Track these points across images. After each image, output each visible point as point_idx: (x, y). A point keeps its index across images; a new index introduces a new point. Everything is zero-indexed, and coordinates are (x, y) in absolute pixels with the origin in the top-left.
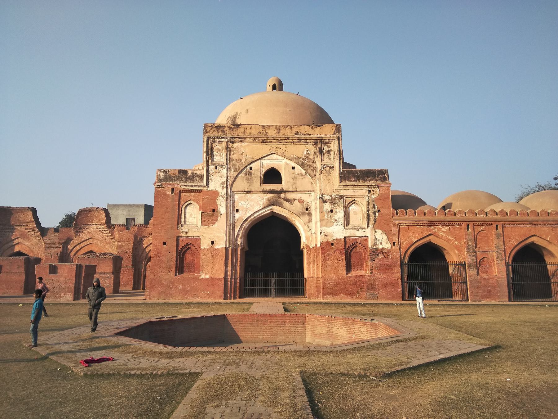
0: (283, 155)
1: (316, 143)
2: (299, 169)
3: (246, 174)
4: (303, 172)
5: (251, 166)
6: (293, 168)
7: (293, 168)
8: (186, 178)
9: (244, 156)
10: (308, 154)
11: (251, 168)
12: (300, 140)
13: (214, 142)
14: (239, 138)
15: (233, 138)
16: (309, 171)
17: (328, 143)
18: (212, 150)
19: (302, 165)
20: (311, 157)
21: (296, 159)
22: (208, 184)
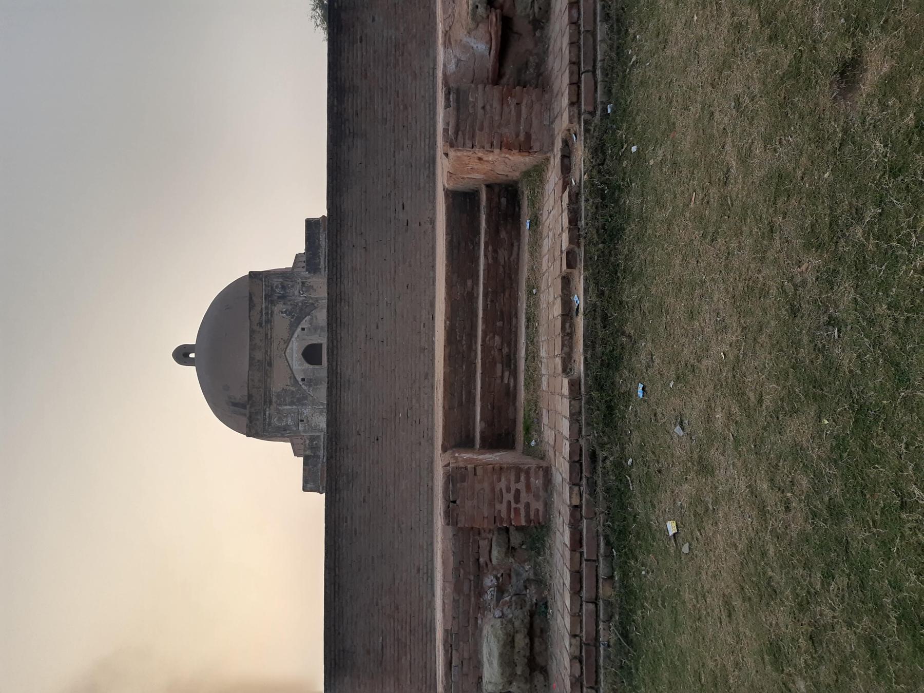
0: (288, 342)
1: (272, 303)
2: (305, 324)
3: (310, 386)
4: (307, 318)
5: (300, 380)
6: (303, 329)
7: (303, 329)
8: (313, 457)
9: (288, 388)
10: (285, 312)
11: (303, 380)
12: (268, 321)
13: (270, 424)
14: (265, 394)
15: (265, 402)
16: (307, 310)
17: (272, 288)
18: (279, 427)
19: (299, 320)
20: (290, 308)
21: (293, 327)
22: (322, 430)
